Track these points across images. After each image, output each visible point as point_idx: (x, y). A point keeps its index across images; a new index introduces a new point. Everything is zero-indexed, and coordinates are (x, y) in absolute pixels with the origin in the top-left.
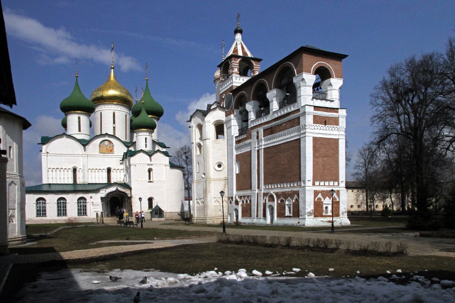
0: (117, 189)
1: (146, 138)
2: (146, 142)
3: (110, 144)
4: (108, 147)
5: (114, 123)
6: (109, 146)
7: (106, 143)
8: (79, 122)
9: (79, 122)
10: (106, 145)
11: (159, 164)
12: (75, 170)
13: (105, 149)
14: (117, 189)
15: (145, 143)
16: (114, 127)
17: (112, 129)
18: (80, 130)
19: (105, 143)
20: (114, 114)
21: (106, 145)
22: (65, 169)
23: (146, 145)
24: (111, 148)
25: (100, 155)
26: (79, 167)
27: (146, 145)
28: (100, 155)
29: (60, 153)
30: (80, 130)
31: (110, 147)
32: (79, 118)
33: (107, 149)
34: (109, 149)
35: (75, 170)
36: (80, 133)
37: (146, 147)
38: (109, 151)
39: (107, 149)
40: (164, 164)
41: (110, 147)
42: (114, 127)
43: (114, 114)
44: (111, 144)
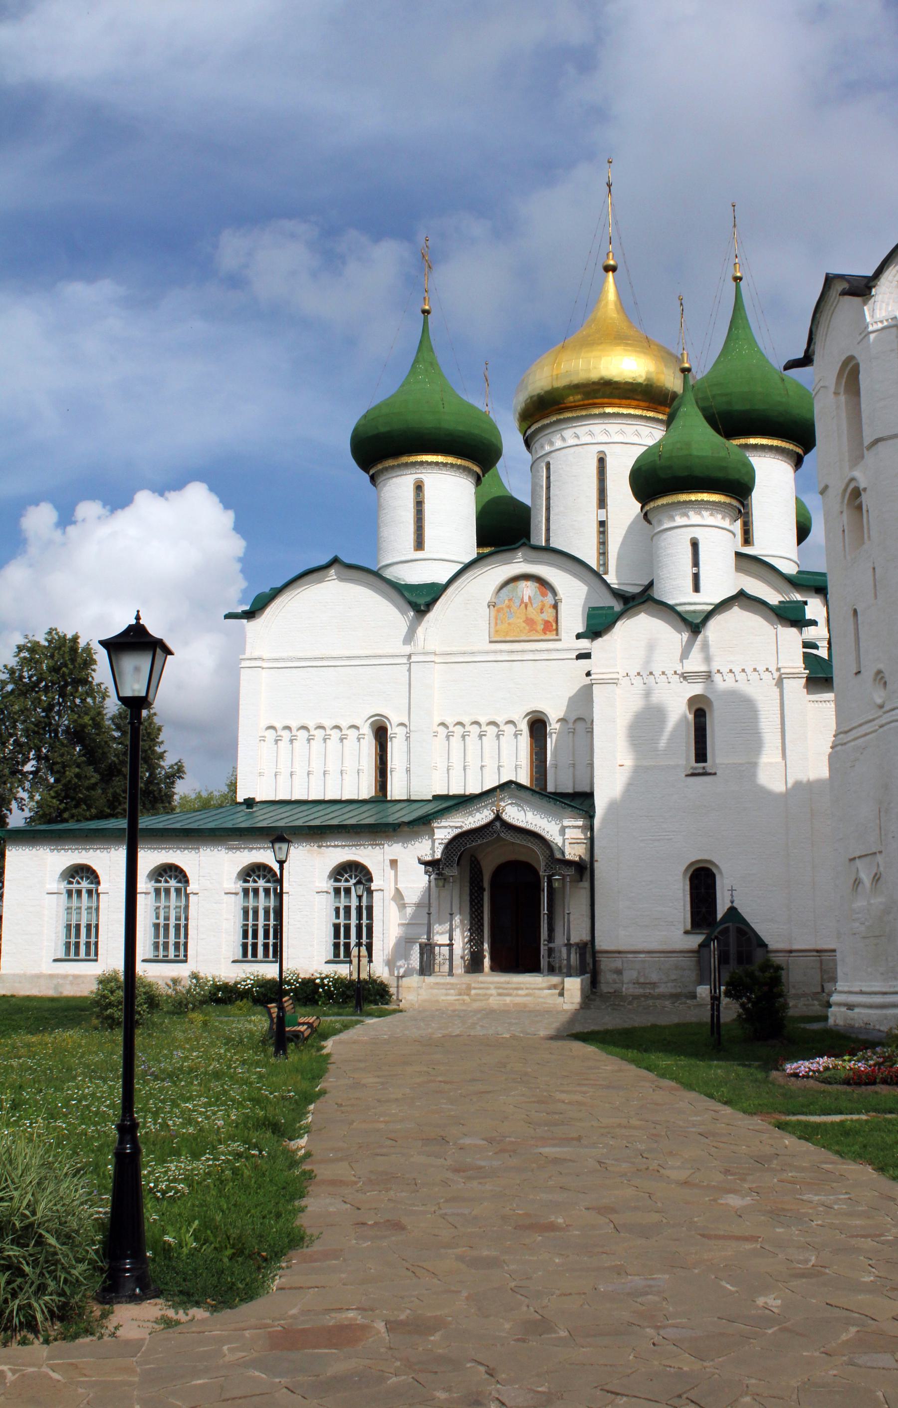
0: (498, 818)
1: (695, 545)
2: (696, 563)
3: (544, 595)
4: (532, 612)
5: (602, 502)
6: (537, 604)
7: (528, 589)
8: (419, 505)
9: (419, 505)
10: (526, 599)
11: (749, 670)
12: (381, 733)
13: (520, 621)
14: (498, 818)
15: (689, 570)
16: (602, 524)
17: (594, 528)
18: (419, 544)
19: (520, 594)
20: (602, 461)
21: (526, 599)
22: (337, 727)
23: (696, 577)
24: (549, 615)
25: (495, 652)
26: (394, 718)
27: (696, 577)
28: (495, 652)
29: (317, 654)
30: (419, 544)
31: (542, 611)
32: (419, 488)
33: (530, 622)
34: (539, 618)
35: (381, 733)
36: (419, 555)
37: (697, 589)
38: (540, 627)
39: (530, 622)
40: (773, 669)
41: (542, 611)
42: (602, 524)
43: (602, 461)
44: (550, 595)
